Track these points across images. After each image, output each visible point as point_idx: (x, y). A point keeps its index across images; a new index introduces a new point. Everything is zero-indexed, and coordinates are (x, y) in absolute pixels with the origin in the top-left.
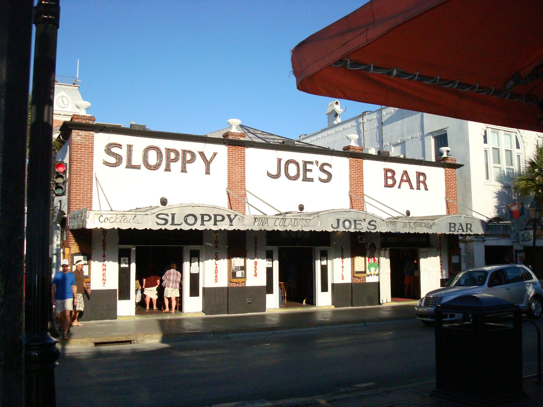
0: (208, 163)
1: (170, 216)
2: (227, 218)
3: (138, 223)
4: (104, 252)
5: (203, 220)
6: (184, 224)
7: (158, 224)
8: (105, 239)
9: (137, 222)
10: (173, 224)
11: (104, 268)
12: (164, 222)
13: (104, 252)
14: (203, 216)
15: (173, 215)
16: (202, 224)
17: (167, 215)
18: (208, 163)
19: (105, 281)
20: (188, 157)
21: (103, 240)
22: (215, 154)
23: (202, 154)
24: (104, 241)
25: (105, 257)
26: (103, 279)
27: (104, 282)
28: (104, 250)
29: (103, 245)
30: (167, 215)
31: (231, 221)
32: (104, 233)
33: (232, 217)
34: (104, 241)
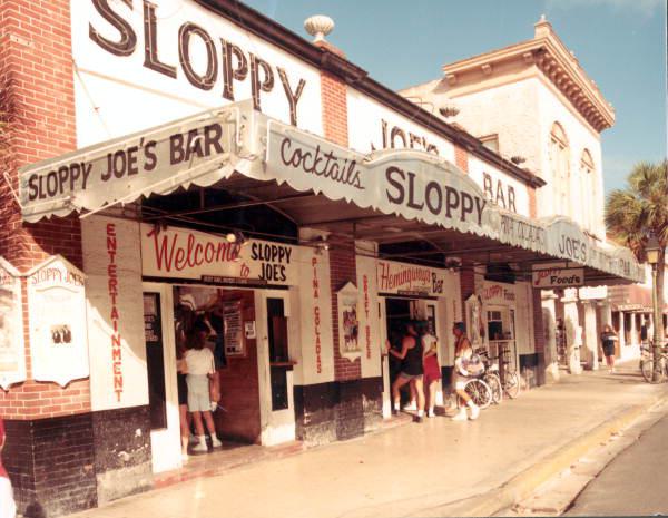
0: (293, 100)
1: (407, 177)
2: (474, 201)
3: (358, 186)
4: (114, 302)
5: (449, 206)
6: (425, 206)
7: (391, 199)
8: (114, 266)
9: (356, 182)
10: (411, 204)
11: (116, 348)
12: (395, 193)
13: (114, 302)
14: (450, 190)
15: (412, 176)
16: (448, 215)
17: (402, 173)
18: (293, 100)
19: (121, 385)
20: (262, 77)
21: (110, 266)
22: (302, 82)
23: (284, 77)
24: (111, 270)
25: (117, 317)
26: (116, 378)
27: (118, 388)
28: (114, 295)
29: (111, 281)
30: (402, 173)
31: (480, 211)
32: (111, 249)
33: (481, 203)
34: (111, 270)
